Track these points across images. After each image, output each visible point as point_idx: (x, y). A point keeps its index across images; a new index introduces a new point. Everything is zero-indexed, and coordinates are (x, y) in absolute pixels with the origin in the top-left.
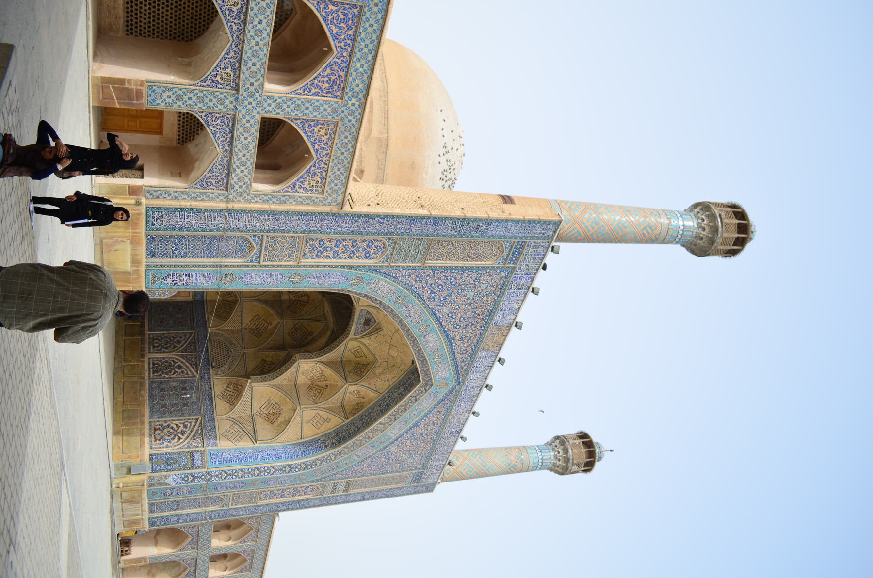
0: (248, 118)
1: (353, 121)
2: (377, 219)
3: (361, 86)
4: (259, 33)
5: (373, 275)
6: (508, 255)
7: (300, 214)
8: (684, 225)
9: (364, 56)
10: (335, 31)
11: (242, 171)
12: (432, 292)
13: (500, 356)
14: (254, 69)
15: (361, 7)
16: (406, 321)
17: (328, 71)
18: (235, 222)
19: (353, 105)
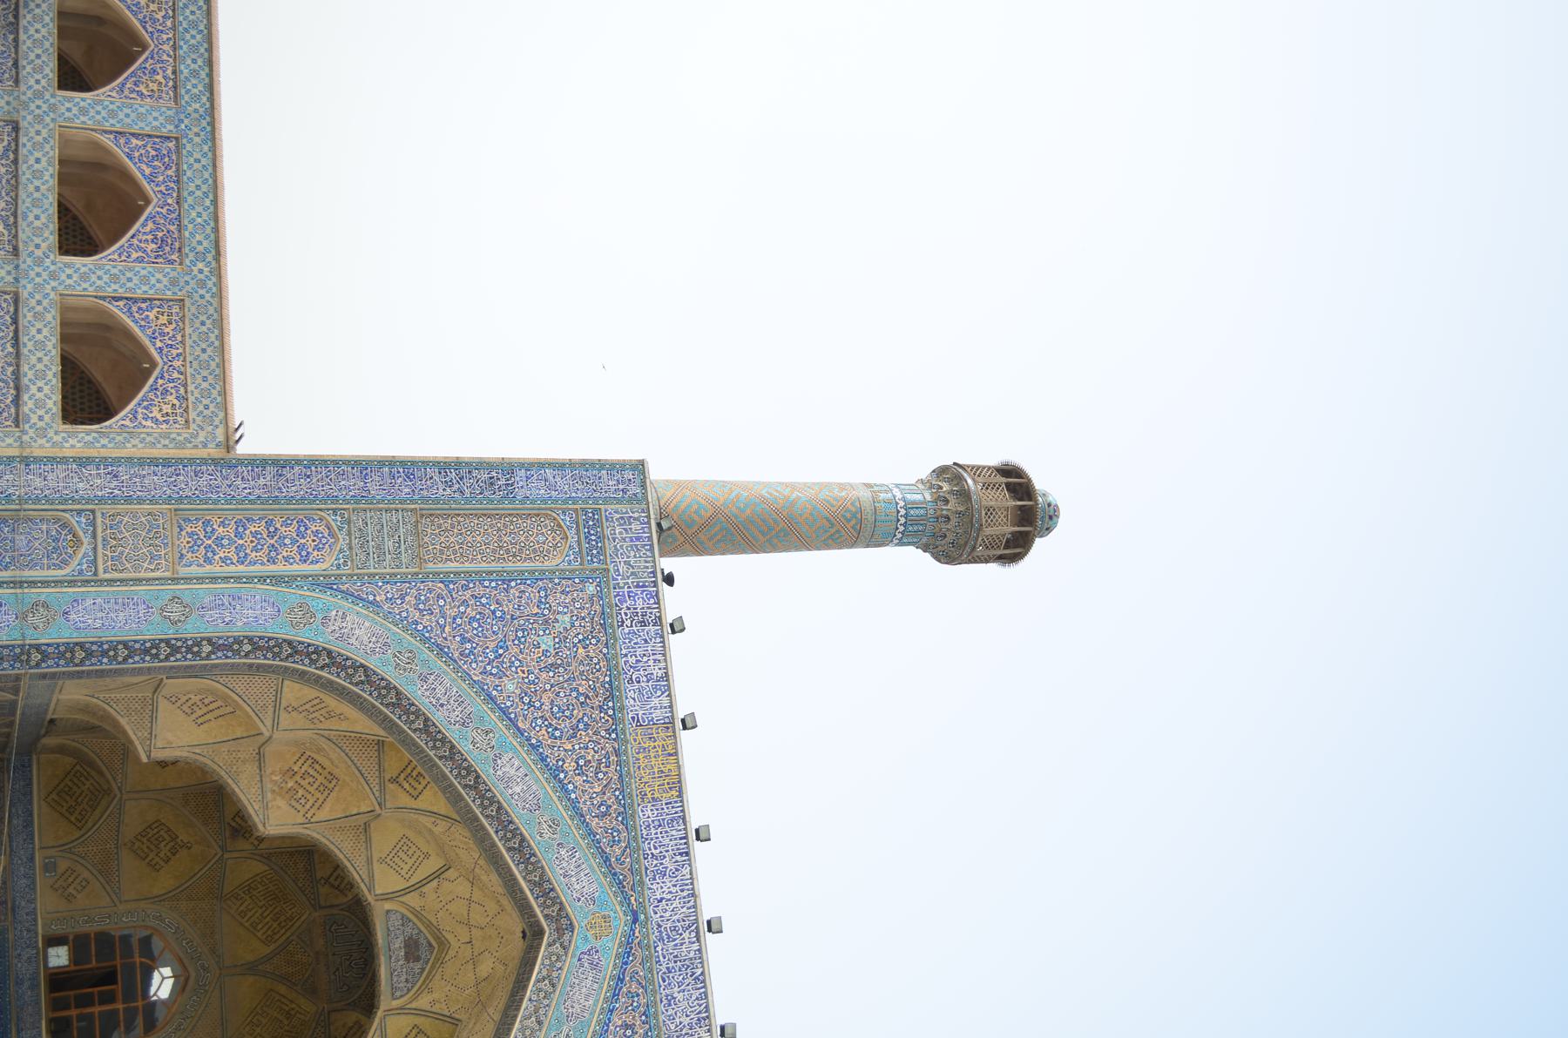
0: (38, 297)
1: (208, 296)
2: (297, 469)
3: (205, 244)
4: (37, 175)
5: (327, 597)
6: (579, 542)
7: (154, 462)
8: (904, 499)
9: (199, 201)
10: (147, 171)
11: (40, 389)
12: (464, 640)
13: (694, 823)
14: (37, 223)
15: (177, 139)
16: (438, 717)
17: (150, 225)
18: (38, 482)
19: (201, 271)
